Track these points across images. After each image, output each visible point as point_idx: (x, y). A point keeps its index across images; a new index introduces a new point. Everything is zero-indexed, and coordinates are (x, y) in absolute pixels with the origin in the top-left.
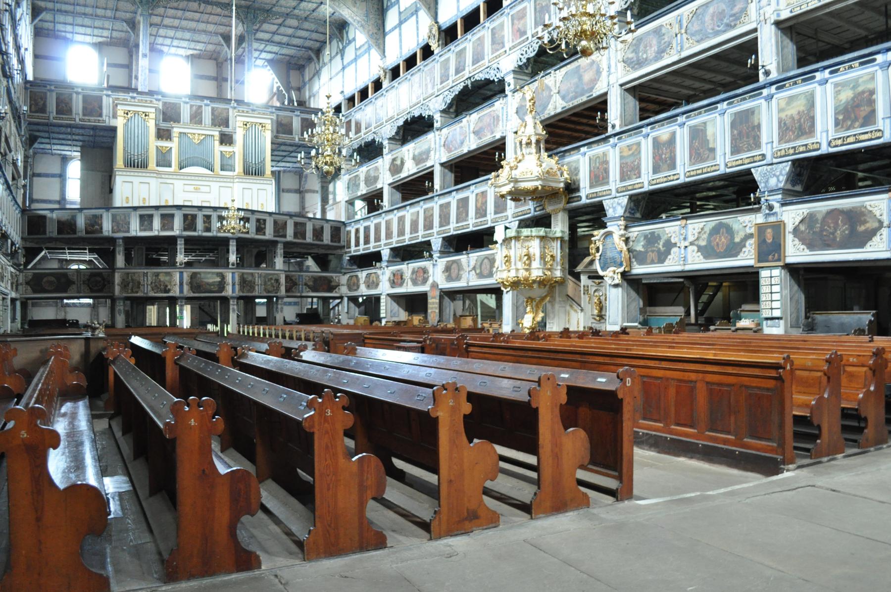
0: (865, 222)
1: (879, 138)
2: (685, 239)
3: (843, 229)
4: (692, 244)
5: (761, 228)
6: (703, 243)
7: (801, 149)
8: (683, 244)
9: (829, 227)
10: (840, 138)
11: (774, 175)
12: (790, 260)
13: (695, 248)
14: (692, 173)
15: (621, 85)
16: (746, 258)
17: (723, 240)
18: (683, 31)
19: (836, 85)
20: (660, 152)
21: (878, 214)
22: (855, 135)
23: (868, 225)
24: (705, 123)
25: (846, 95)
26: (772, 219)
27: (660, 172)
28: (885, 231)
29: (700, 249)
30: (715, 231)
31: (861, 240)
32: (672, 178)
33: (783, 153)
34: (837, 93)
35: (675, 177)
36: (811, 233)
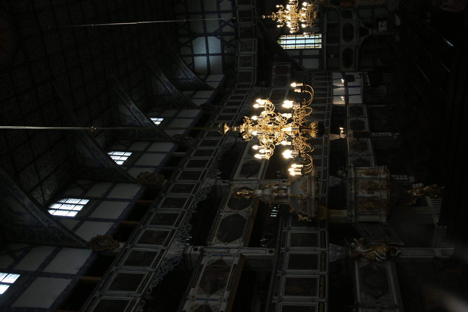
12: (368, 130)
15: (261, 178)
28: (360, 119)
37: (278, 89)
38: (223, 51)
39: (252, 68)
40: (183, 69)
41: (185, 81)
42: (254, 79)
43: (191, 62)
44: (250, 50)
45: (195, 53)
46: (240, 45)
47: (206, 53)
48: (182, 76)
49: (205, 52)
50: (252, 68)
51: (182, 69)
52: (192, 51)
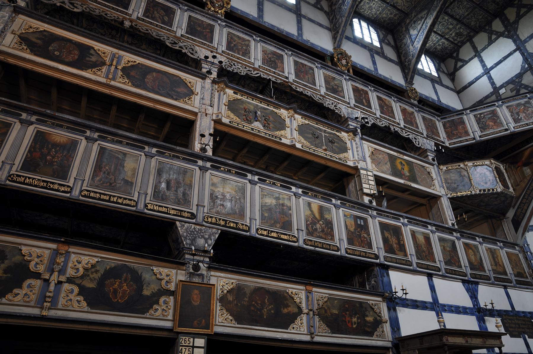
0: (287, 306)
1: (295, 242)
2: (62, 272)
3: (268, 309)
4: (70, 280)
5: (185, 287)
6: (90, 285)
7: (232, 225)
8: (54, 278)
9: (257, 304)
10: (266, 230)
11: (203, 237)
12: (218, 329)
13: (76, 290)
14: (92, 195)
16: (161, 317)
17: (123, 289)
18: (120, 67)
19: (262, 189)
20: (45, 150)
21: (298, 301)
22: (277, 233)
23: (290, 309)
24: (125, 154)
25: (270, 201)
26: (196, 280)
27: (34, 171)
28: (304, 317)
29: (83, 291)
30: (114, 273)
31: (286, 322)
32: (56, 187)
33: (214, 220)
34: (263, 196)
35: (63, 189)
36: (242, 306)
37: (434, 175)
38: (502, 87)
39: (478, 133)
40: (424, 26)
41: (409, 41)
42: (455, 143)
43: (467, 59)
44: (516, 121)
45: (482, 54)
46: (523, 101)
47: (489, 66)
48: (413, 32)
49: (489, 65)
50: (478, 133)
51: (422, 25)
52: (483, 50)
